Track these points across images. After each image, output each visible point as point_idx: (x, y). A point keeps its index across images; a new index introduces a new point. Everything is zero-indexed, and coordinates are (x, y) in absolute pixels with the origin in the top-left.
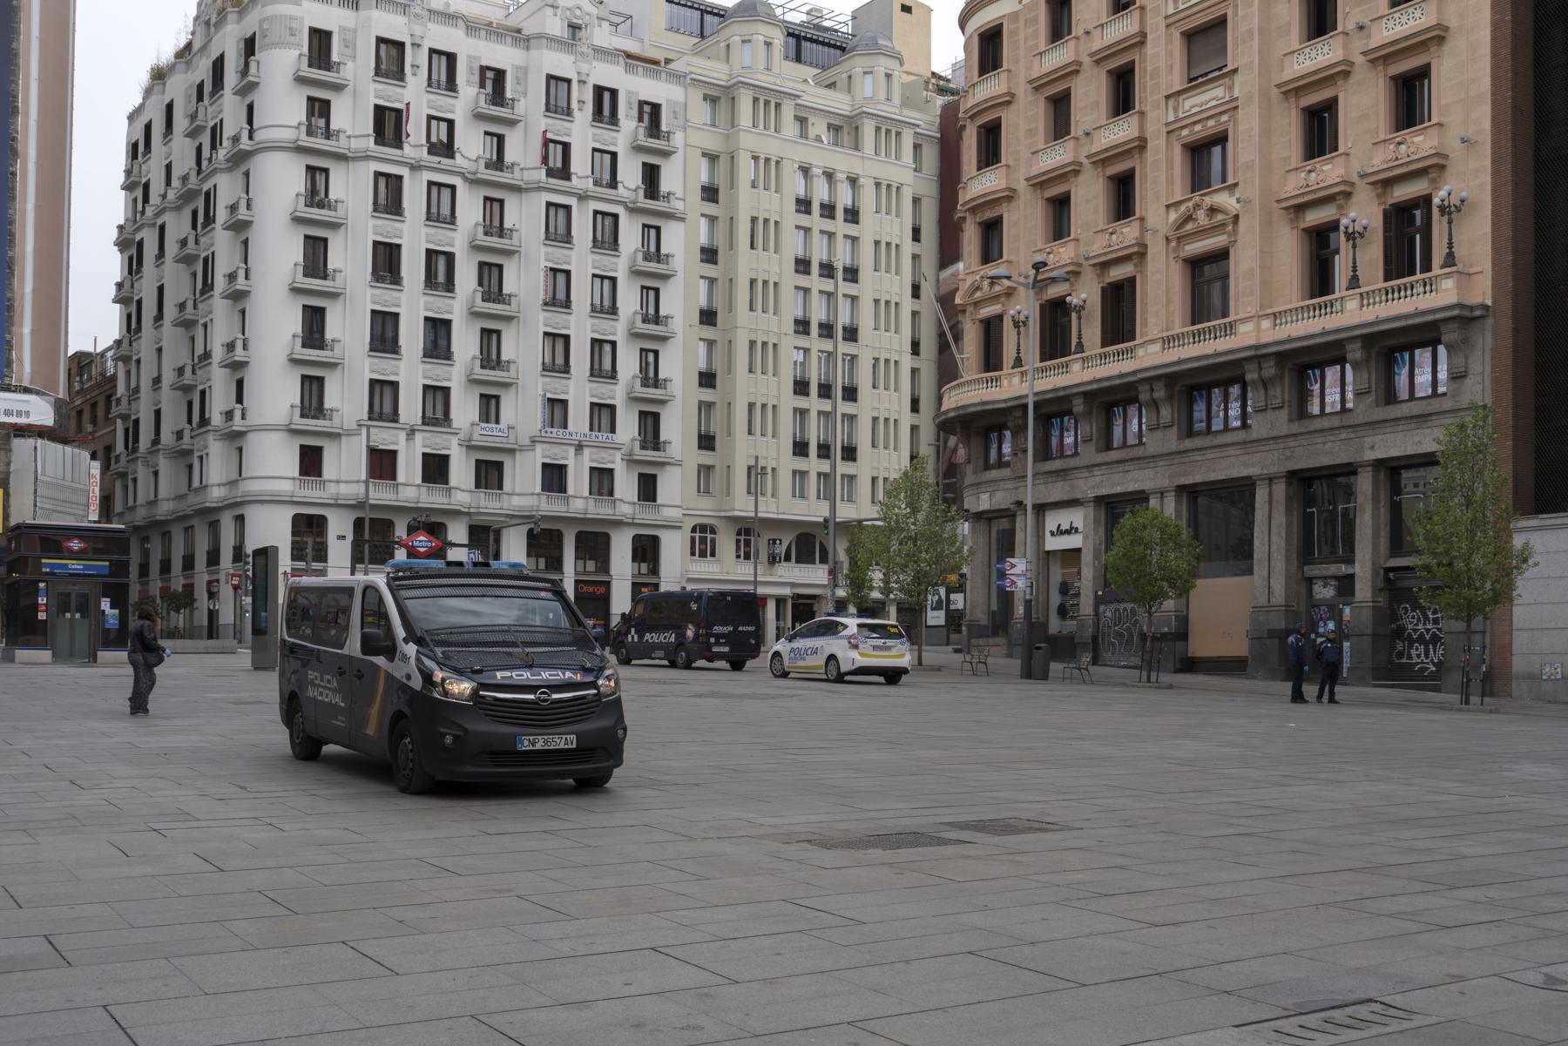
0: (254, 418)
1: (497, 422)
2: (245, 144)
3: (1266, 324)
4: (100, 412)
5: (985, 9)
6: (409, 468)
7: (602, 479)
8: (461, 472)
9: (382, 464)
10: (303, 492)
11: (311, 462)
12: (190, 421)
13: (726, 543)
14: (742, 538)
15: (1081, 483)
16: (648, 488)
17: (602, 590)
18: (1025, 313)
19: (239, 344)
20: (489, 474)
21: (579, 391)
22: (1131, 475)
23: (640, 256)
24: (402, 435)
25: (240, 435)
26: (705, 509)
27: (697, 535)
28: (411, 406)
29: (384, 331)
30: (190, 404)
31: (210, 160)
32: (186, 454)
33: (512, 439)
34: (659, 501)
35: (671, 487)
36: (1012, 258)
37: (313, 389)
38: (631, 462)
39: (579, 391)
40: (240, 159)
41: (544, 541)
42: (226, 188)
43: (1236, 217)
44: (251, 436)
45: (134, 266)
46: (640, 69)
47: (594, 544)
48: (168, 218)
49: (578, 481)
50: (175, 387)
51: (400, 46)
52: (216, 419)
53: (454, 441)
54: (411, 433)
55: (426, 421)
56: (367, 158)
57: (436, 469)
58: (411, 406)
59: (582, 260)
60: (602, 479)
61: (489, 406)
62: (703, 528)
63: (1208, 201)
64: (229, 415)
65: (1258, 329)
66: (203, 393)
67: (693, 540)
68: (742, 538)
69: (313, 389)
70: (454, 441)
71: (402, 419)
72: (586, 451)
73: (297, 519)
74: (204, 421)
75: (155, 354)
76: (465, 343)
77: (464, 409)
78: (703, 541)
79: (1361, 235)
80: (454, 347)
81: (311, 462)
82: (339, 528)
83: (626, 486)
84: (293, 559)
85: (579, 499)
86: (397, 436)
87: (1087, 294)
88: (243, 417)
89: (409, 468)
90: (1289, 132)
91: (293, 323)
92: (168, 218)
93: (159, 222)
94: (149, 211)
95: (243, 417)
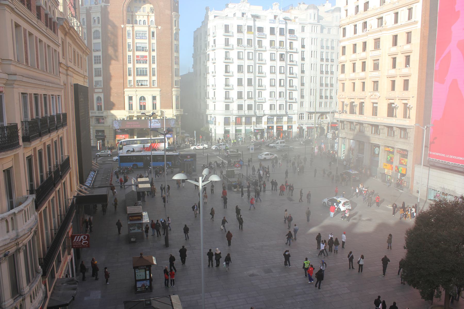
1: (261, 97)
6: (245, 107)
9: (240, 107)
11: (227, 107)
29: (240, 82)
41: (270, 119)
52: (211, 98)
55: (248, 98)
57: (250, 107)
62: (302, 114)
64: (213, 98)
67: (299, 116)
68: (309, 115)
73: (225, 118)
78: (302, 116)
82: (233, 119)
89: (245, 107)
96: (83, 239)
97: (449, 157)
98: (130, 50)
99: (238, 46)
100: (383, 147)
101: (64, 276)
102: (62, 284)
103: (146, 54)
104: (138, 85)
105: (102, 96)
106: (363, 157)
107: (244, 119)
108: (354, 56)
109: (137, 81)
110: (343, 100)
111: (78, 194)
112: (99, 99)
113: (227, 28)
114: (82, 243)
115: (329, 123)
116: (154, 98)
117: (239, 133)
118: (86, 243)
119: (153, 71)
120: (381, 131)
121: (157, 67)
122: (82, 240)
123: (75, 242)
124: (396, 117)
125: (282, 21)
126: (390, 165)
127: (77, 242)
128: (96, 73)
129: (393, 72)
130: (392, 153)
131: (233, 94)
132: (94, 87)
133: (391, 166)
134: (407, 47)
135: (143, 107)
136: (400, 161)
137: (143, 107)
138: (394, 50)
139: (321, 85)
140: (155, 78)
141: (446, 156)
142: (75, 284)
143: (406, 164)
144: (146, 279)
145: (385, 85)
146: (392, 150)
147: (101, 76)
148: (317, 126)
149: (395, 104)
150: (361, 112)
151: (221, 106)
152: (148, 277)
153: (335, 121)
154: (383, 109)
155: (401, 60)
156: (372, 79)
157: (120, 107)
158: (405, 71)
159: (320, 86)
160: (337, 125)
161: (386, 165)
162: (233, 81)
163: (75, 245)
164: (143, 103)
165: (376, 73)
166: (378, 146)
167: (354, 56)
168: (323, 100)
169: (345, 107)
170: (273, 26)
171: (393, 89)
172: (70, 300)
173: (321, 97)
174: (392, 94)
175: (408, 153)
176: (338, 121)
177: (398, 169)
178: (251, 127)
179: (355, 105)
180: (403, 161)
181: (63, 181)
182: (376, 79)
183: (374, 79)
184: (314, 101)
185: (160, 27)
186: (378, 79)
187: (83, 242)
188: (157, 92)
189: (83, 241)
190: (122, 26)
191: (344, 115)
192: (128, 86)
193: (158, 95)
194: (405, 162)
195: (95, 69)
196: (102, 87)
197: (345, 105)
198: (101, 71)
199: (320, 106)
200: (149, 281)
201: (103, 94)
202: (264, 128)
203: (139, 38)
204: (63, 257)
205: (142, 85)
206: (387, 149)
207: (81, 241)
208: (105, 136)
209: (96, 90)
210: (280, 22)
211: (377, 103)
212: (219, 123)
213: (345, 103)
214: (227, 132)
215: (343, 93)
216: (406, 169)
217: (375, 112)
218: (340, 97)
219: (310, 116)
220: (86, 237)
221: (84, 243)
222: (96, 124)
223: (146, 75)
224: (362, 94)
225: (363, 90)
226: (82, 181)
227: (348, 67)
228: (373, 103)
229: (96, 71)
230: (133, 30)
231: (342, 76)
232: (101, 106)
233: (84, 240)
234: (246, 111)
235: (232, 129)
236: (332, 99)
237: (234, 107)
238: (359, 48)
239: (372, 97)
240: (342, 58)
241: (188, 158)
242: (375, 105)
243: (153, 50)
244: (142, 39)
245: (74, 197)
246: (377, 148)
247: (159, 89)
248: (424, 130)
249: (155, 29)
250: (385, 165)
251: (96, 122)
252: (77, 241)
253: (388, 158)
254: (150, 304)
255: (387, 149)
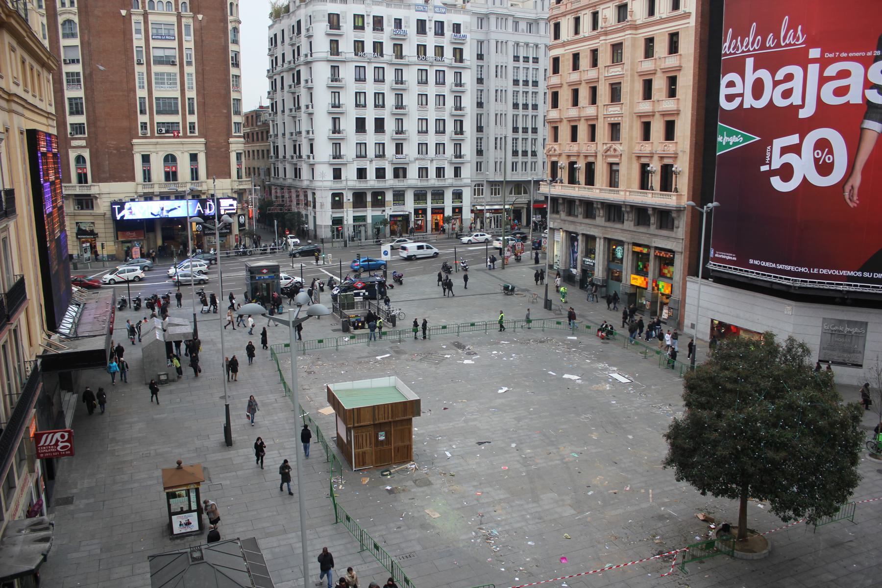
0: (317, 159)
1: (402, 154)
2: (309, 59)
3: (628, 193)
4: (265, 137)
5: (557, 49)
6: (371, 174)
7: (440, 172)
8: (389, 174)
9: (362, 173)
10: (335, 185)
11: (337, 174)
12: (295, 152)
13: (486, 189)
14: (493, 188)
15: (578, 227)
16: (457, 172)
17: (441, 211)
18: (564, 165)
19: (311, 132)
20: (400, 172)
21: (432, 139)
22: (592, 229)
23: (454, 85)
24: (368, 162)
25: (314, 164)
26: (480, 178)
27: (477, 188)
28: (371, 152)
29: (361, 125)
30: (294, 98)
31: (298, 58)
32: (294, 117)
33: (407, 159)
34: (462, 176)
35: (467, 172)
36: (561, 142)
37: (337, 146)
38: (451, 163)
39: (432, 139)
40: (308, 63)
41: (420, 196)
42: (304, 71)
43: (621, 154)
44: (316, 165)
45: (274, 84)
46: (453, 11)
47: (438, 194)
48: (285, 74)
49: (432, 173)
50: (288, 92)
51: (363, 16)
52: (304, 157)
53: (387, 162)
54: (371, 161)
55: (376, 157)
56: (352, 61)
57: (380, 173)
58: (371, 152)
59: (432, 90)
60: (440, 172)
61: (399, 148)
62: (479, 185)
63: (614, 146)
64: (309, 157)
65: (625, 195)
66: (298, 96)
67: (475, 189)
68: (493, 188)
69: (337, 146)
70: (387, 162)
71: (368, 157)
72: (434, 162)
74: (300, 157)
75: (282, 124)
76: (390, 126)
77: (390, 150)
78: (479, 189)
79: (654, 173)
80: (385, 128)
81: (337, 174)
82: (348, 197)
83: (449, 172)
84: (332, 209)
85: (432, 180)
86: (366, 163)
87: (581, 165)
88: (313, 159)
89: (371, 174)
90: (638, 132)
91: (329, 125)
92: (285, 74)
93: (282, 75)
94: (279, 69)
95: (313, 159)
96: (61, 440)
97: (819, 271)
98: (142, 62)
99: (356, 55)
100: (630, 246)
101: (22, 515)
102: (20, 531)
103: (175, 70)
104: (160, 132)
105: (86, 154)
106: (594, 264)
107: (369, 199)
108: (575, 77)
109: (158, 123)
110: (554, 159)
111: (45, 351)
112: (80, 159)
113: (334, 21)
114: (59, 448)
115: (530, 202)
116: (194, 157)
117: (361, 223)
118: (66, 447)
119: (189, 104)
120: (626, 215)
121: (197, 95)
122: (57, 441)
123: (43, 446)
124: (653, 190)
125: (439, 8)
126: (643, 278)
127: (48, 445)
128: (71, 108)
129: (646, 107)
130: (648, 254)
131: (349, 150)
132: (69, 136)
133: (645, 280)
134: (672, 61)
135: (171, 176)
136: (661, 270)
137: (171, 176)
138: (648, 65)
139: (515, 130)
140: (193, 118)
141: (809, 270)
142: (47, 529)
143: (671, 275)
144: (190, 511)
145: (631, 130)
146: (645, 251)
147: (82, 113)
148: (507, 207)
149: (651, 165)
150: (590, 180)
151: (325, 174)
152: (194, 506)
153: (543, 198)
154: (629, 174)
155: (660, 85)
156: (609, 119)
157: (124, 175)
158: (669, 105)
159: (513, 132)
160: (545, 206)
161: (637, 279)
162: (348, 125)
163: (45, 453)
164: (172, 168)
165: (614, 109)
166: (620, 243)
167: (575, 77)
168: (520, 159)
169: (559, 171)
170: (422, 16)
171: (646, 136)
172: (38, 561)
173: (515, 153)
174: (647, 148)
175: (674, 255)
176: (546, 198)
177: (657, 286)
178: (384, 211)
179: (577, 168)
180: (666, 271)
181: (13, 327)
182: (616, 119)
183: (612, 119)
184: (503, 161)
185: (200, 17)
186: (620, 118)
187: (61, 445)
188: (198, 145)
189: (59, 443)
190: (124, 12)
191: (557, 187)
192: (140, 135)
193: (202, 151)
194: (669, 272)
195: (70, 99)
196: (86, 136)
197: (560, 168)
198: (82, 104)
199: (513, 171)
200: (196, 513)
201: (88, 150)
202: (407, 213)
203: (160, 37)
204: (19, 478)
205: (167, 132)
206: (637, 249)
207: (56, 444)
208: (97, 234)
209: (74, 143)
210: (437, 10)
211: (618, 164)
212: (322, 205)
213: (559, 164)
214: (338, 222)
215: (556, 147)
216: (672, 285)
217: (613, 182)
218: (551, 152)
219: (495, 189)
220: (66, 434)
221: (61, 448)
222: (75, 211)
223: (176, 112)
224: (592, 148)
225: (593, 139)
226: (52, 323)
227: (565, 97)
228: (611, 164)
229: (71, 104)
230: (146, 22)
231: (554, 114)
232: (86, 175)
233: (62, 442)
234: (371, 183)
235: (348, 214)
236: (536, 155)
237: (349, 174)
238: (585, 62)
239: (609, 153)
240: (555, 80)
241: (263, 273)
242: (615, 168)
243: (189, 63)
244: (166, 39)
245: (37, 357)
246: (619, 248)
247: (203, 140)
248: (702, 214)
249: (191, 20)
250: (634, 279)
251: (76, 207)
252: (46, 444)
253: (638, 266)
254: (202, 558)
255: (637, 249)
